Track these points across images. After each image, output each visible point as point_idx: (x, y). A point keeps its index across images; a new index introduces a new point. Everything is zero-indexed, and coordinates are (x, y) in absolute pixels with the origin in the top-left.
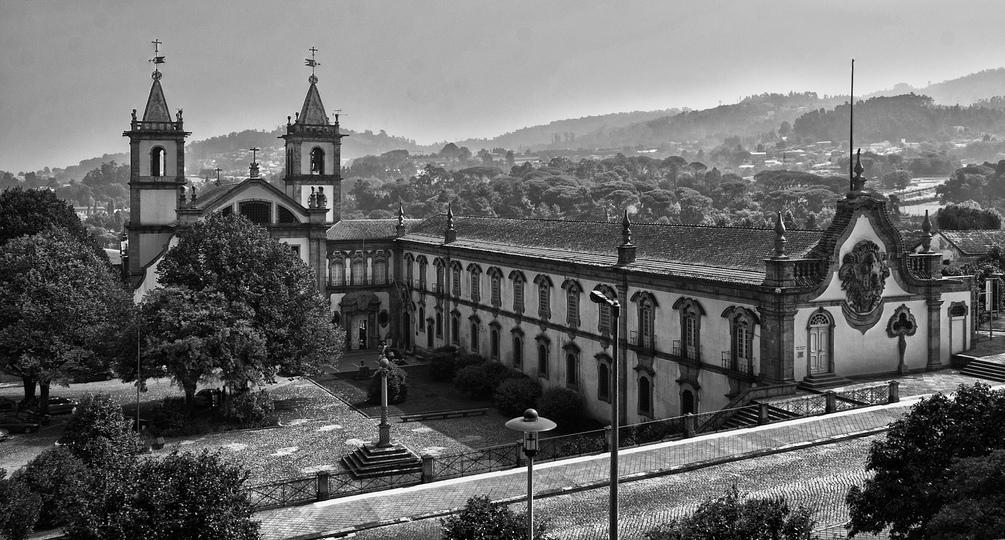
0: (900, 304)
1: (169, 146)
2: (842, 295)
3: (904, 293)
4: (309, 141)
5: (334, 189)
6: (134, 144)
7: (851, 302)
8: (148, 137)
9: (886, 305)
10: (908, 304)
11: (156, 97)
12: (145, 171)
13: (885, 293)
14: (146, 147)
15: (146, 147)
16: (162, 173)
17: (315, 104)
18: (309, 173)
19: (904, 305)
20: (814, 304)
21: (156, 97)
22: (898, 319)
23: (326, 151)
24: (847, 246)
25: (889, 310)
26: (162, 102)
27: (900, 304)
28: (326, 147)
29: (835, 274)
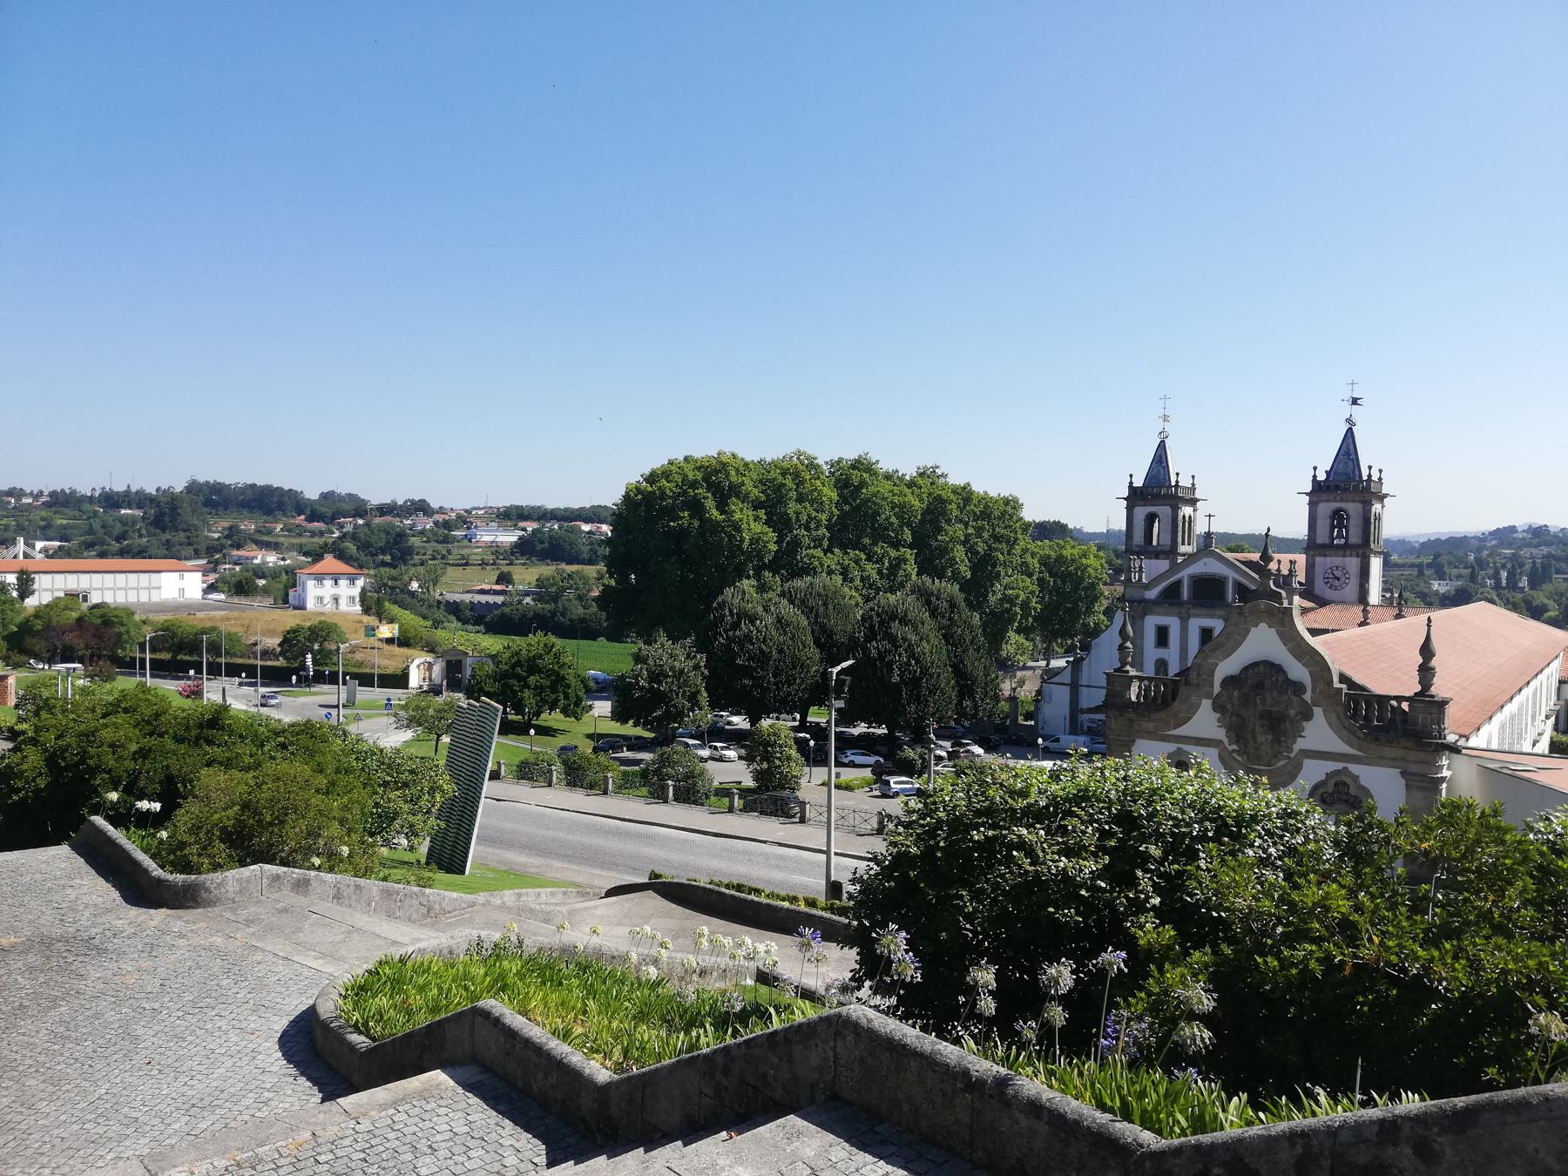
0: (1339, 766)
1: (1164, 511)
2: (1220, 734)
3: (1342, 747)
4: (1328, 501)
5: (1362, 562)
6: (1130, 509)
7: (1234, 747)
8: (1143, 503)
9: (1308, 764)
10: (1355, 769)
11: (1160, 458)
12: (1138, 538)
13: (1300, 744)
14: (1141, 512)
15: (1141, 512)
16: (1155, 543)
17: (1348, 453)
18: (1327, 541)
19: (1345, 769)
20: (1166, 739)
21: (1160, 458)
22: (1330, 788)
23: (1351, 512)
24: (1228, 666)
25: (1314, 772)
26: (1164, 464)
27: (1339, 766)
28: (1353, 508)
29: (1206, 704)
